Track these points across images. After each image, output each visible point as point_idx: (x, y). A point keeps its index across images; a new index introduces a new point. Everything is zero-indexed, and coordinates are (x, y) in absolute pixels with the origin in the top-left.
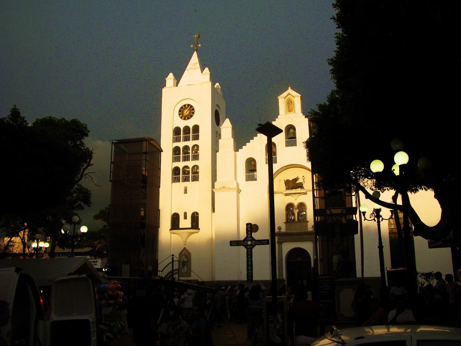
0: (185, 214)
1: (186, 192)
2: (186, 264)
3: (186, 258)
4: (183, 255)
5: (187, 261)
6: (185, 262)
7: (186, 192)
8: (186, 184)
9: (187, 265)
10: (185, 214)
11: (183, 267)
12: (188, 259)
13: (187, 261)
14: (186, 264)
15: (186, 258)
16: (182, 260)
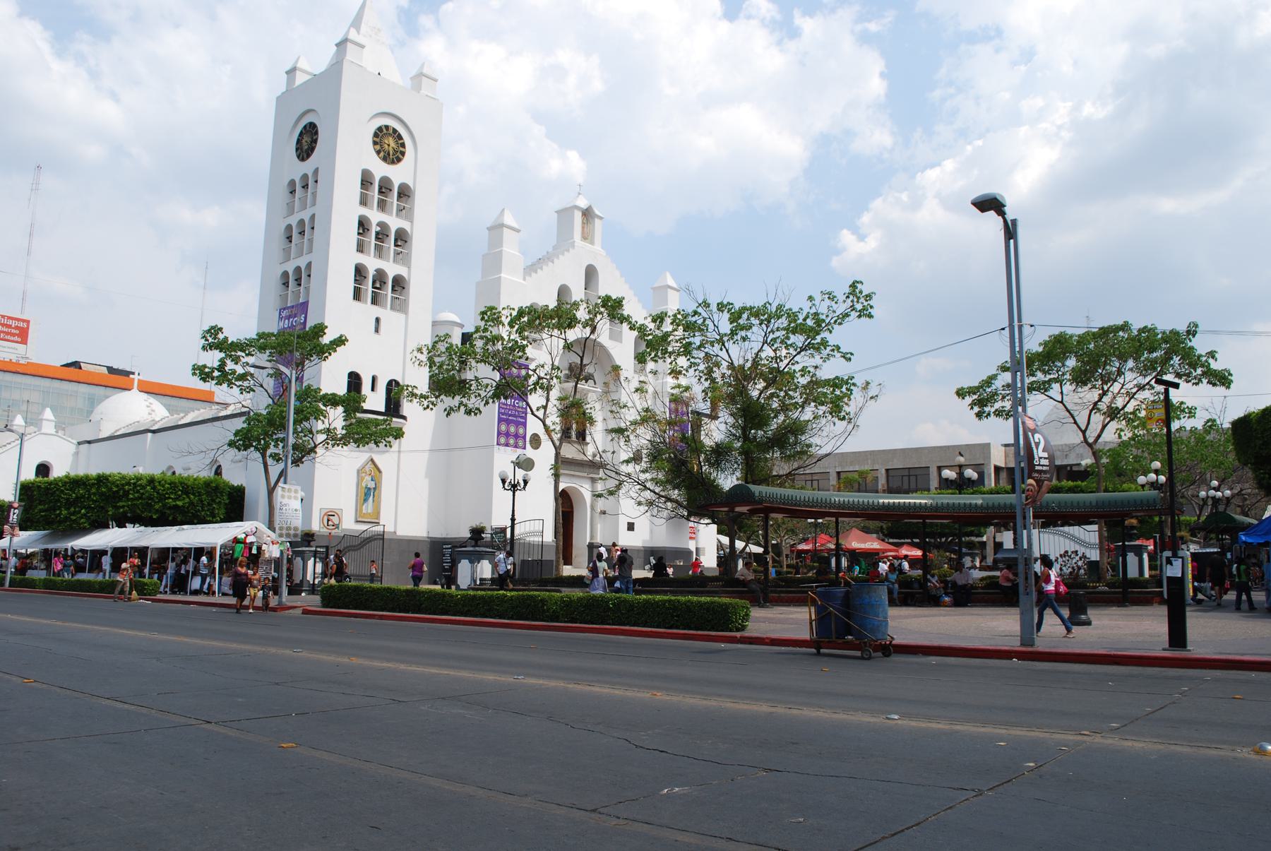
0: (374, 379)
1: (377, 330)
2: (372, 494)
3: (372, 480)
4: (366, 473)
5: (375, 489)
6: (369, 489)
7: (377, 330)
8: (376, 311)
9: (374, 495)
10: (374, 379)
11: (365, 500)
12: (376, 484)
13: (375, 489)
14: (372, 494)
15: (372, 480)
16: (364, 485)
